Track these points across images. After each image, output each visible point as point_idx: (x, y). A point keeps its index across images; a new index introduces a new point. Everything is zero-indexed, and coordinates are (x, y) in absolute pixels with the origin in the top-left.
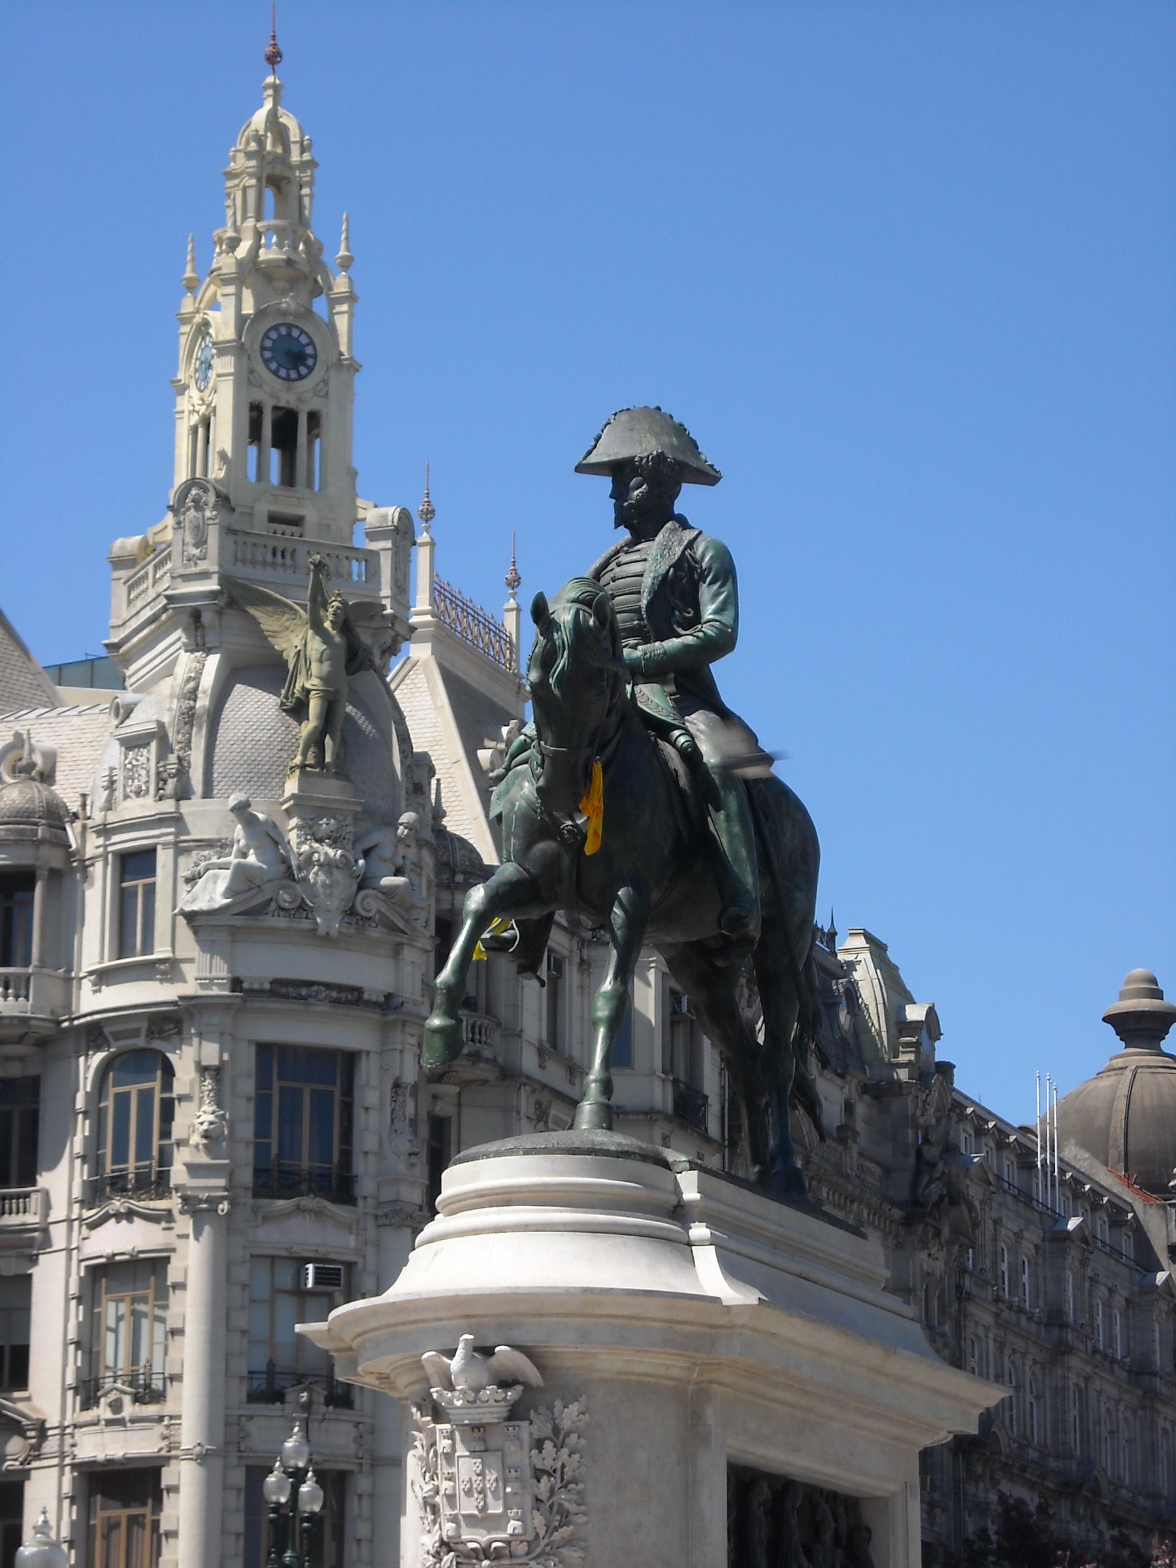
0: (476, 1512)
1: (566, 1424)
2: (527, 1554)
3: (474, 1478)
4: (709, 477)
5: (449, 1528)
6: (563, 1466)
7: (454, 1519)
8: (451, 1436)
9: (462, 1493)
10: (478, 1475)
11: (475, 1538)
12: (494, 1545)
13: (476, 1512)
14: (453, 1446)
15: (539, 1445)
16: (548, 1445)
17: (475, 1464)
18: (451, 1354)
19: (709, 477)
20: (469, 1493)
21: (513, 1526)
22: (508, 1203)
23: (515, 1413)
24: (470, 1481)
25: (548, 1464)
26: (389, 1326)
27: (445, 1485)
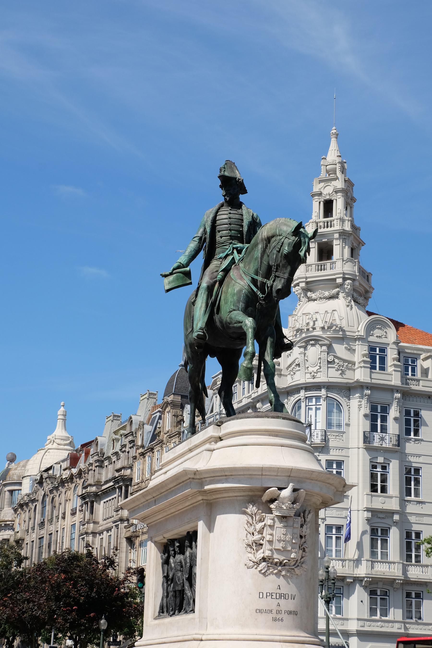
0: (281, 548)
1: (308, 520)
2: (294, 565)
3: (282, 536)
4: (244, 191)
5: (268, 553)
6: (305, 536)
7: (271, 550)
8: (273, 519)
9: (277, 541)
10: (284, 535)
11: (277, 557)
12: (285, 561)
13: (281, 548)
14: (274, 523)
15: (302, 526)
16: (305, 527)
17: (283, 531)
18: (280, 489)
19: (244, 191)
20: (279, 541)
21: (293, 556)
22: (277, 436)
23: (297, 514)
24: (280, 537)
25: (303, 534)
26: (250, 475)
27: (268, 537)
